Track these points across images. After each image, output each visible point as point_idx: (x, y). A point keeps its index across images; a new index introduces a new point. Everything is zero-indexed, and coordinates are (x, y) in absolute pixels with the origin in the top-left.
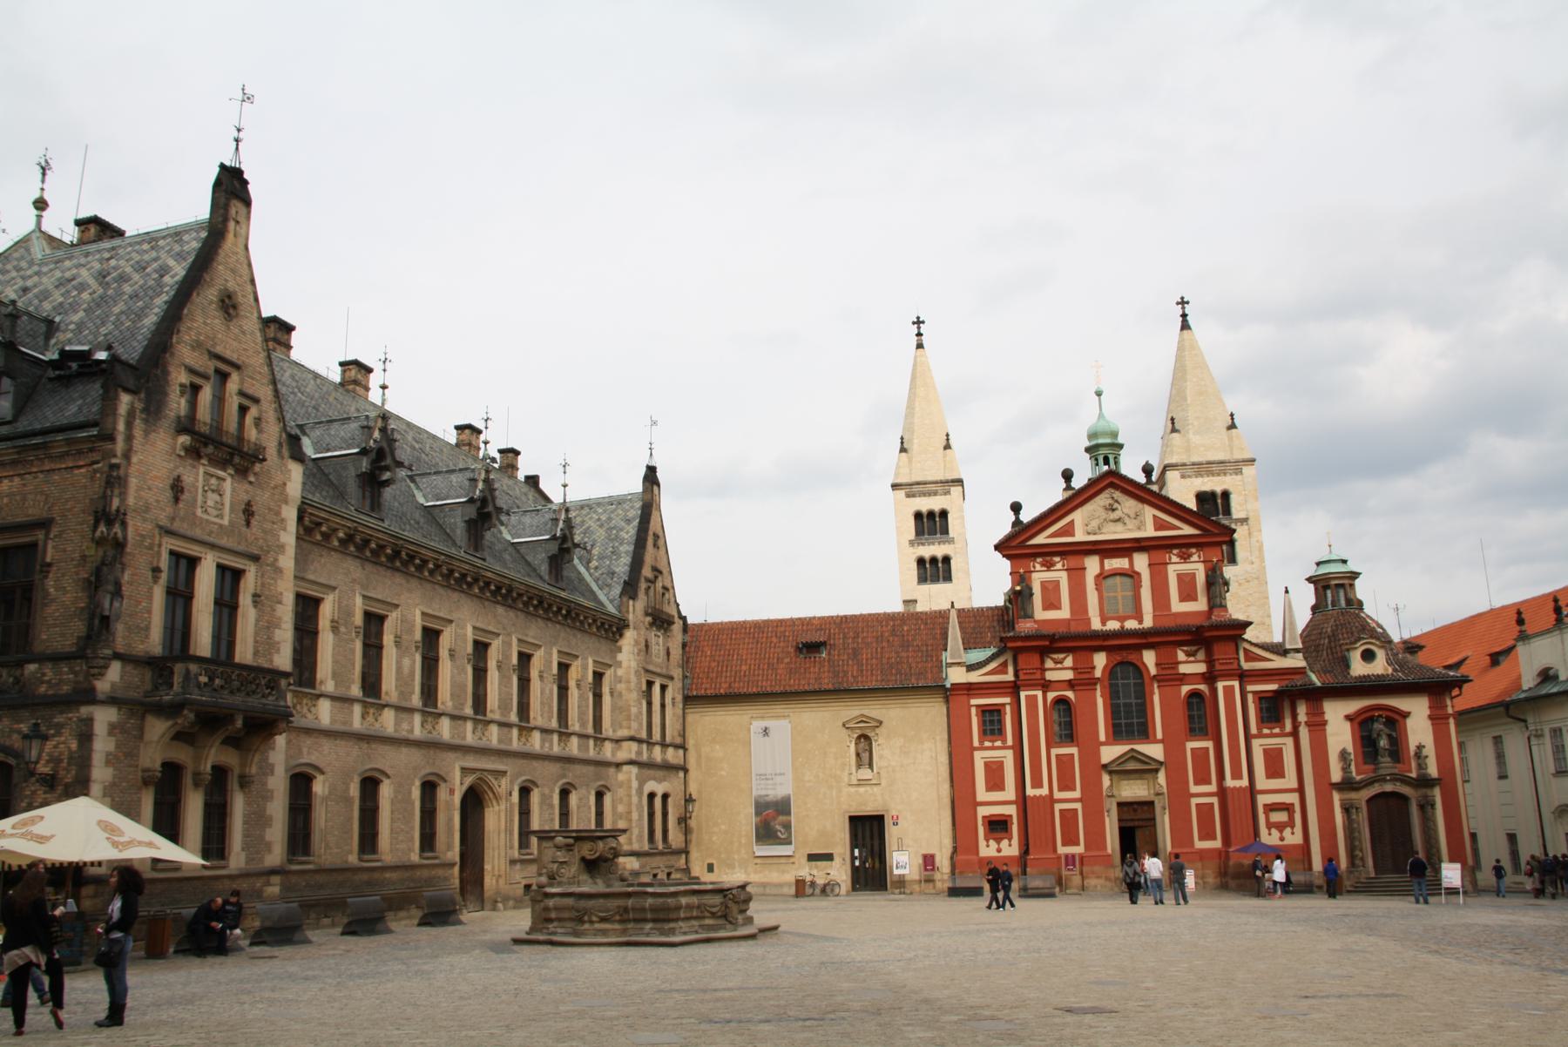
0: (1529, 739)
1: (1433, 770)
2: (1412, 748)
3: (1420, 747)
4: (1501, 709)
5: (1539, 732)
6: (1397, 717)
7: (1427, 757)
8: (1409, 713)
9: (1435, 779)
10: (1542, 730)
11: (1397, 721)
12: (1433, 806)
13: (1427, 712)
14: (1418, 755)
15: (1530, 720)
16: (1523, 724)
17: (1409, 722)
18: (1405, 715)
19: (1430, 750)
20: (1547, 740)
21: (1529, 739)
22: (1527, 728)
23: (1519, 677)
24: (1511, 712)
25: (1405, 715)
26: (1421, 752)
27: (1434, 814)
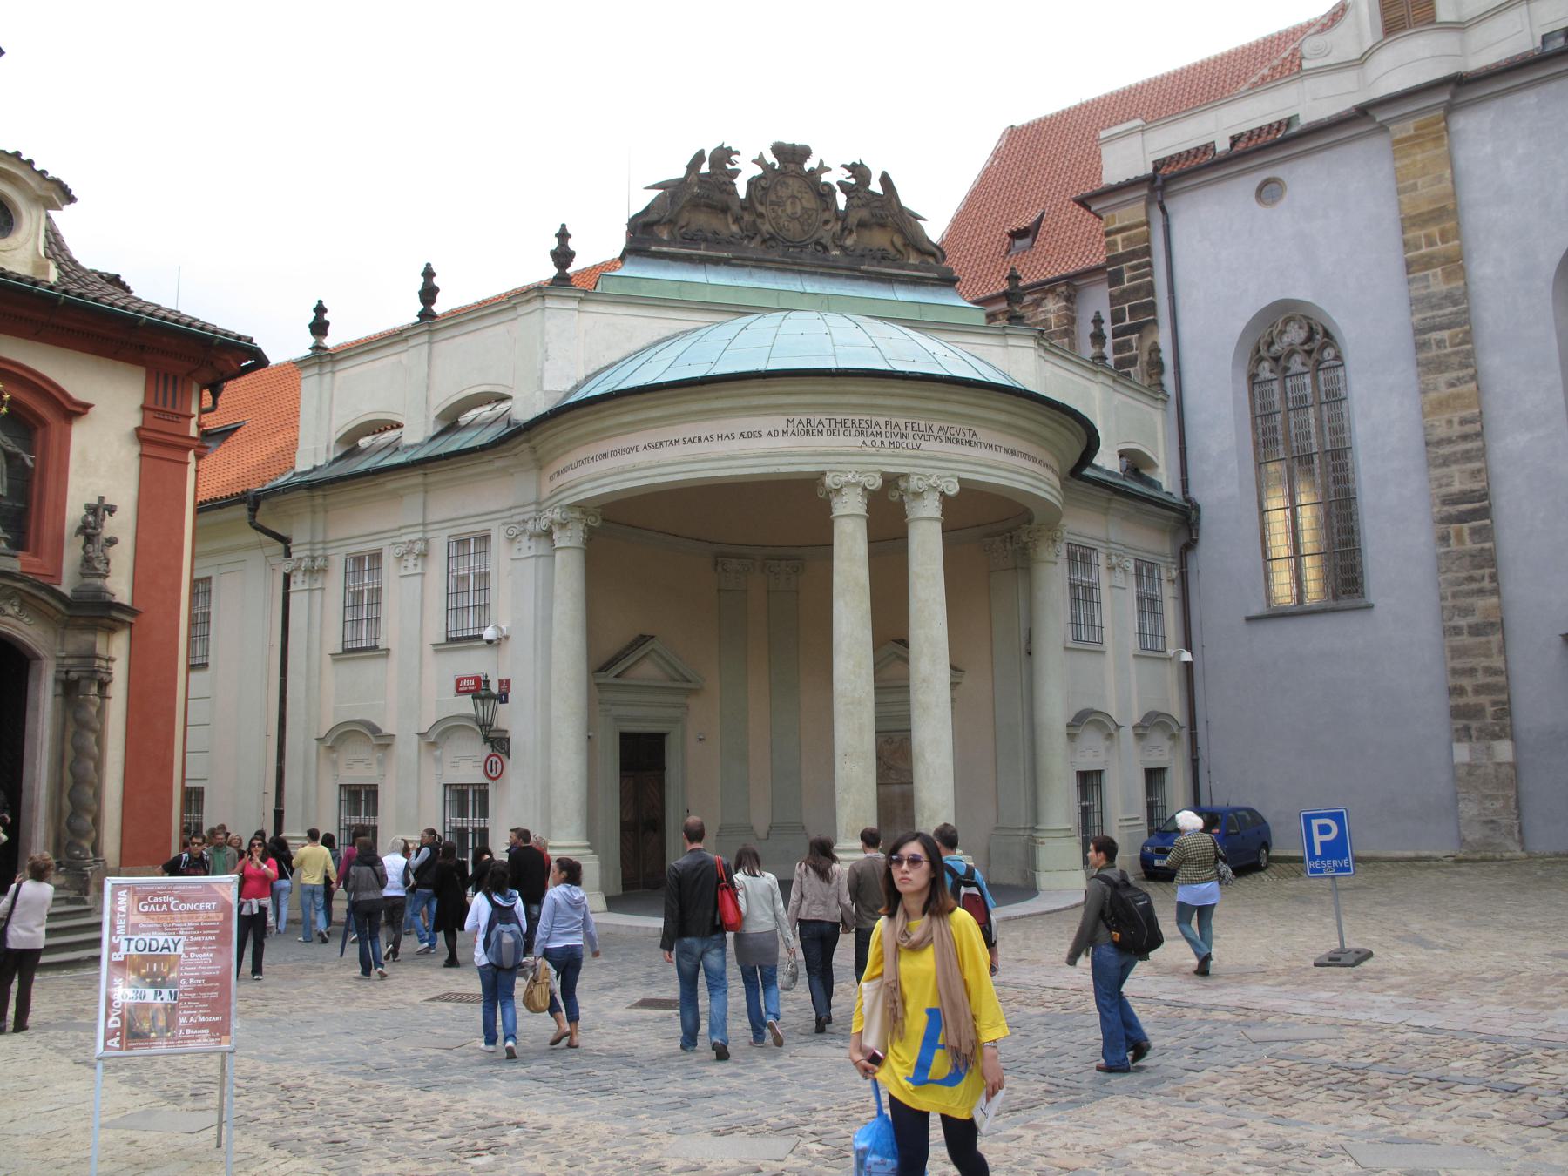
0: (287, 579)
1: (120, 586)
2: (74, 512)
3: (100, 510)
4: (242, 511)
5: (319, 563)
6: (44, 411)
7: (112, 542)
8: (87, 407)
9: (120, 607)
10: (326, 558)
11: (44, 423)
12: (103, 686)
13: (135, 420)
14: (89, 531)
15: (300, 536)
16: (281, 546)
17: (81, 436)
18: (74, 411)
19: (121, 525)
20: (335, 585)
21: (287, 579)
22: (288, 554)
23: (293, 446)
24: (259, 520)
25: (74, 411)
26: (98, 524)
27: (101, 711)
